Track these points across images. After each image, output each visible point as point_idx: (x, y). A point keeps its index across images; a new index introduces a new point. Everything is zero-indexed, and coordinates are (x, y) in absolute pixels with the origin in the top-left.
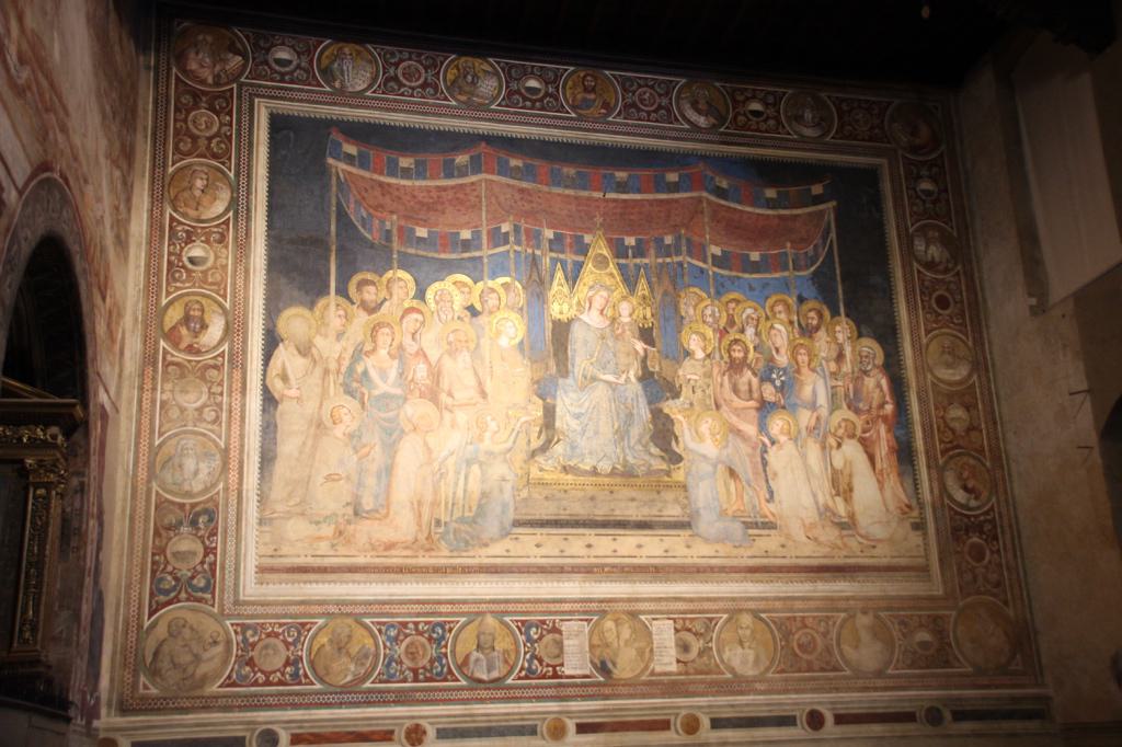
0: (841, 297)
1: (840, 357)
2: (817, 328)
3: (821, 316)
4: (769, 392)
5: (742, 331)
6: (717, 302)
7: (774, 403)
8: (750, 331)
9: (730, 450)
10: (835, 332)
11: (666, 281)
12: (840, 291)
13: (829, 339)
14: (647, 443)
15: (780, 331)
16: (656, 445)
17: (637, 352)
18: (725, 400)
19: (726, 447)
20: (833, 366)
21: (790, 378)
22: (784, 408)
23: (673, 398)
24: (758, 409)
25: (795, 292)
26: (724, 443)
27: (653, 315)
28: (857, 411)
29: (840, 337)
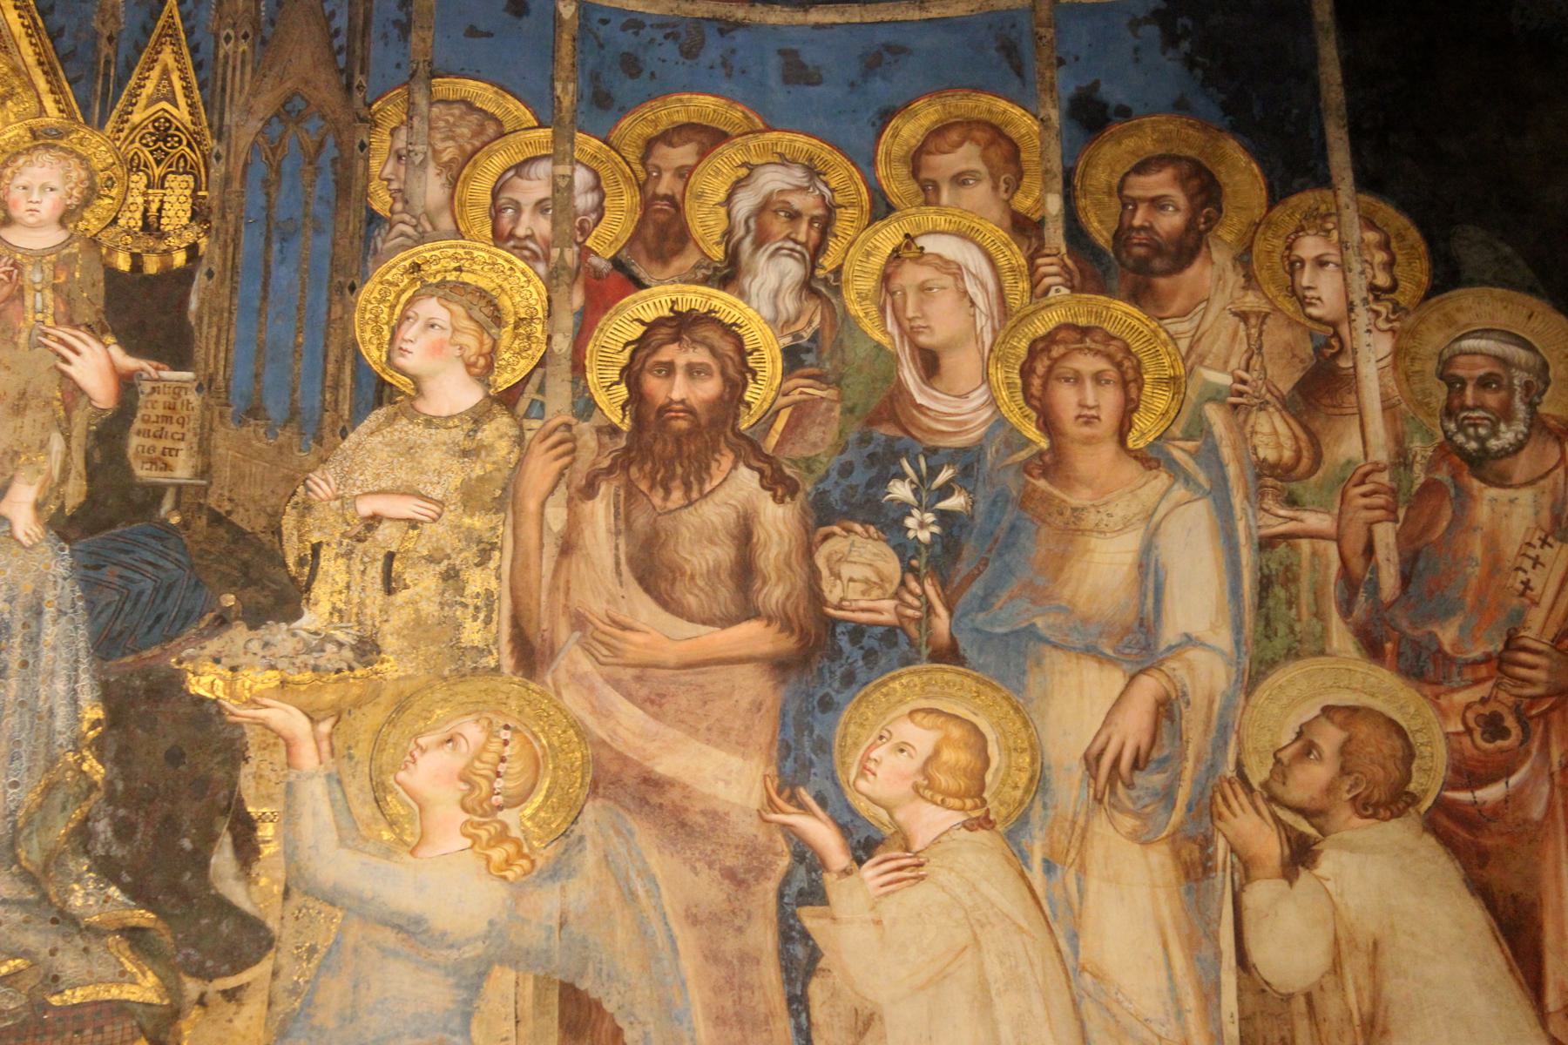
0: (1333, 92)
1: (1322, 385)
2: (1186, 249)
3: (1206, 190)
4: (861, 575)
5: (728, 275)
6: (588, 144)
7: (890, 634)
8: (774, 274)
9: (579, 893)
10: (1294, 266)
11: (303, 59)
12: (1331, 73)
13: (1251, 301)
14: (53, 859)
15: (946, 265)
16: (108, 870)
17: (73, 392)
18: (580, 622)
19: (557, 871)
20: (1273, 435)
21: (1000, 500)
22: (950, 654)
23: (256, 618)
24: (780, 666)
25: (1067, 83)
26: (545, 855)
27: (199, 214)
28: (1425, 667)
29: (1326, 290)
